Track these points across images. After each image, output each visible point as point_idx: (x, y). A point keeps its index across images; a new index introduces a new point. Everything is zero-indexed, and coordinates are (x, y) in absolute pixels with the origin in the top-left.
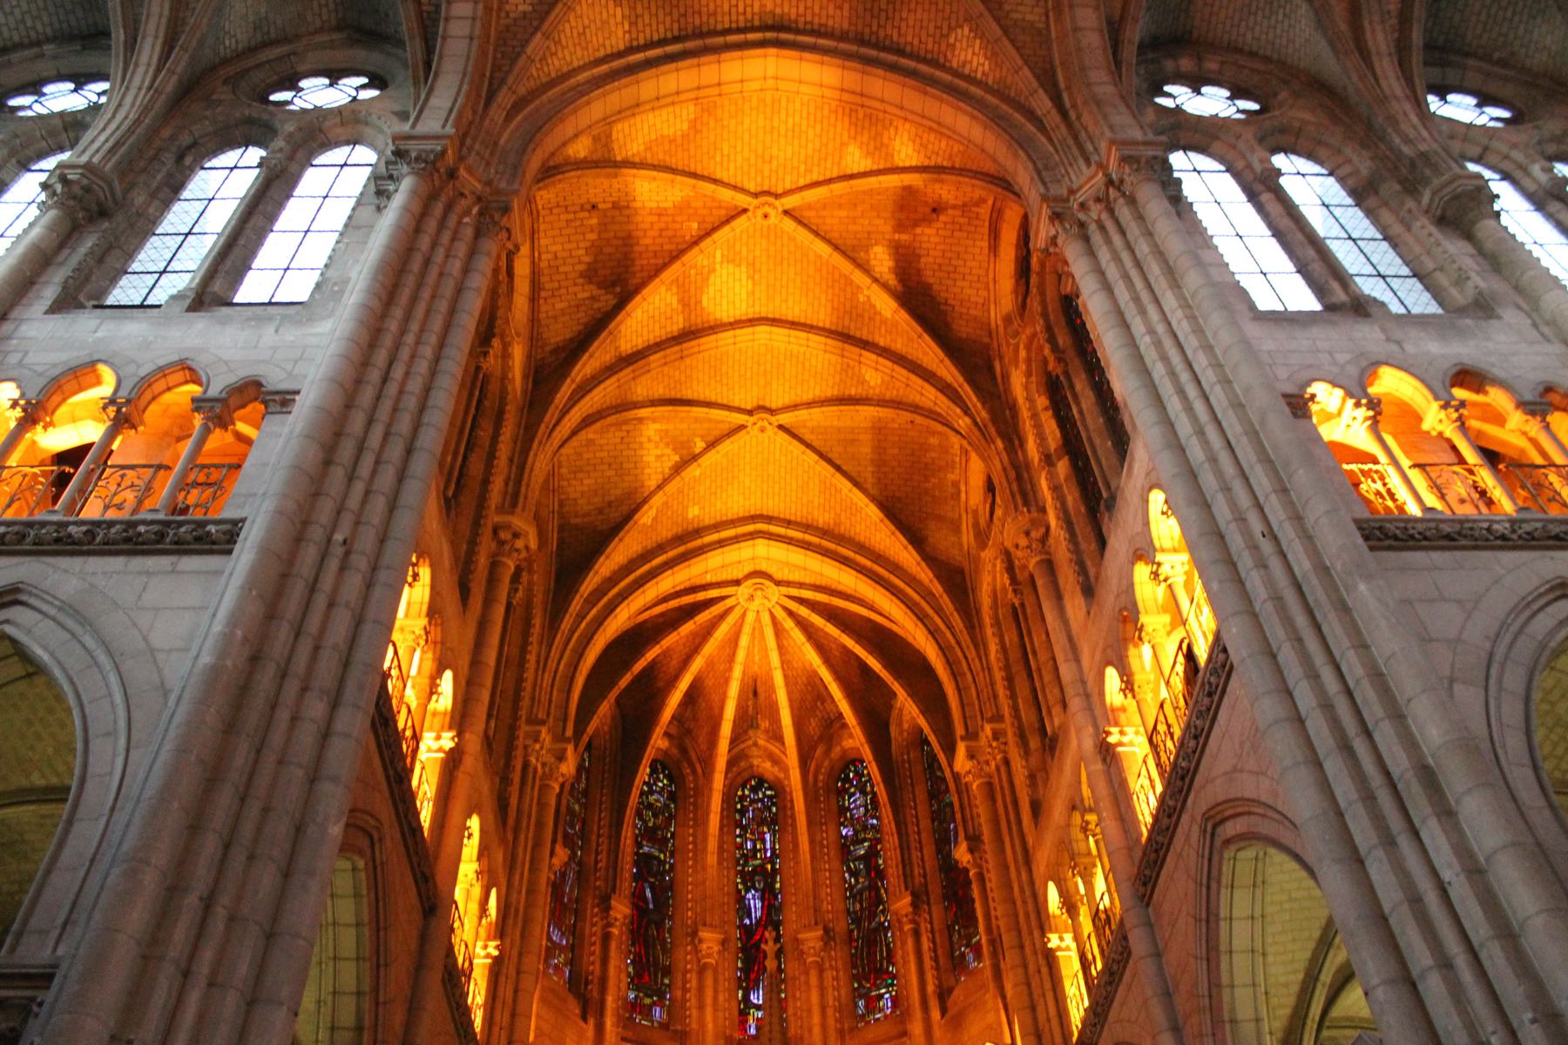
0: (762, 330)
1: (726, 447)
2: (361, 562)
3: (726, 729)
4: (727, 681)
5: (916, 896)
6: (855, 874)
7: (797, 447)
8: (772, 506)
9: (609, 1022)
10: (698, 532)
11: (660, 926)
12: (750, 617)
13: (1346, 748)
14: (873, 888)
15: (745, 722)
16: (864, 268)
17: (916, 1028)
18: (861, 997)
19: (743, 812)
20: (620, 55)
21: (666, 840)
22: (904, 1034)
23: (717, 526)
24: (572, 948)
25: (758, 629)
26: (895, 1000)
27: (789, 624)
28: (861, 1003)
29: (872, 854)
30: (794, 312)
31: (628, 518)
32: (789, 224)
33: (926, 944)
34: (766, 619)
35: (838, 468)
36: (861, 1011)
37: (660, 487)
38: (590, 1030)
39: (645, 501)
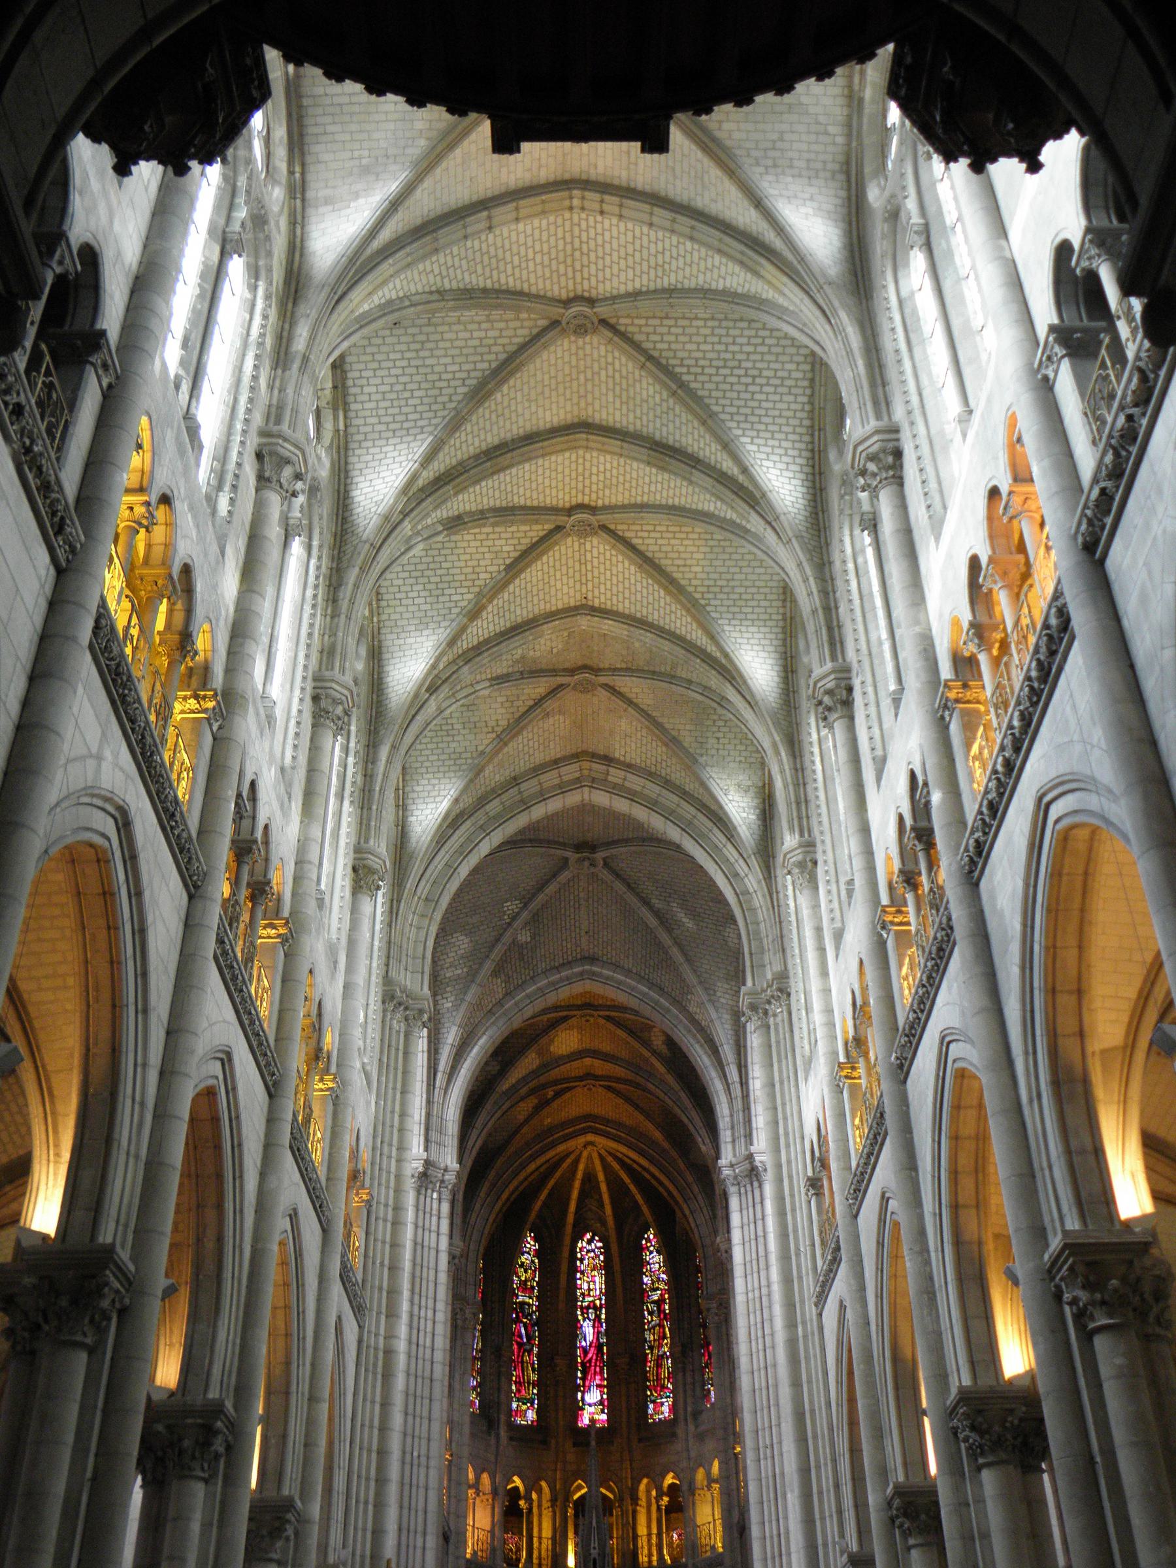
0: (588, 1061)
1: (568, 1095)
2: (423, 1460)
3: (570, 1218)
4: (571, 1187)
5: (683, 1345)
6: (651, 1313)
7: (610, 1095)
8: (596, 1111)
9: (503, 1433)
10: (551, 1130)
11: (530, 1352)
12: (585, 1154)
13: (773, 1558)
14: (661, 1326)
15: (583, 1195)
16: (646, 1044)
17: (680, 1431)
18: (654, 1402)
19: (582, 1260)
20: (500, 1003)
21: (533, 1288)
22: (674, 1435)
23: (564, 1125)
24: (479, 1385)
25: (590, 1158)
26: (673, 1409)
27: (610, 1159)
28: (651, 1406)
29: (659, 1303)
30: (606, 1047)
31: (508, 1142)
32: (602, 1021)
33: (689, 1380)
34: (595, 1155)
35: (637, 1107)
36: (650, 1411)
37: (526, 1121)
38: (493, 1441)
39: (517, 1132)
